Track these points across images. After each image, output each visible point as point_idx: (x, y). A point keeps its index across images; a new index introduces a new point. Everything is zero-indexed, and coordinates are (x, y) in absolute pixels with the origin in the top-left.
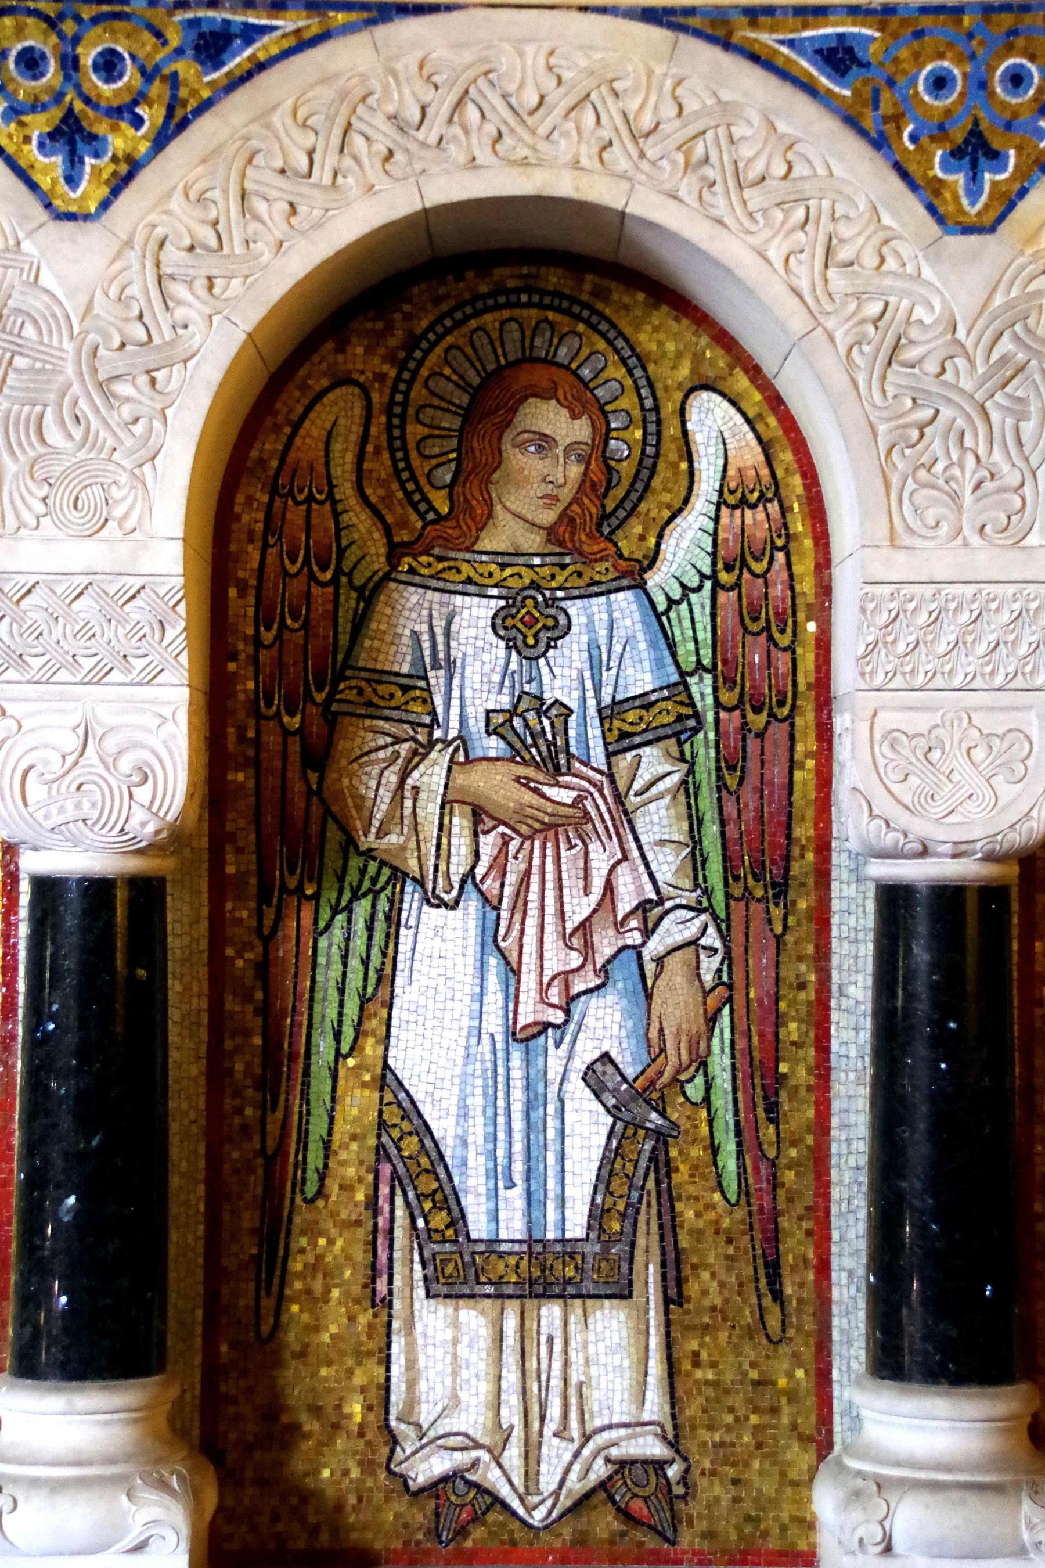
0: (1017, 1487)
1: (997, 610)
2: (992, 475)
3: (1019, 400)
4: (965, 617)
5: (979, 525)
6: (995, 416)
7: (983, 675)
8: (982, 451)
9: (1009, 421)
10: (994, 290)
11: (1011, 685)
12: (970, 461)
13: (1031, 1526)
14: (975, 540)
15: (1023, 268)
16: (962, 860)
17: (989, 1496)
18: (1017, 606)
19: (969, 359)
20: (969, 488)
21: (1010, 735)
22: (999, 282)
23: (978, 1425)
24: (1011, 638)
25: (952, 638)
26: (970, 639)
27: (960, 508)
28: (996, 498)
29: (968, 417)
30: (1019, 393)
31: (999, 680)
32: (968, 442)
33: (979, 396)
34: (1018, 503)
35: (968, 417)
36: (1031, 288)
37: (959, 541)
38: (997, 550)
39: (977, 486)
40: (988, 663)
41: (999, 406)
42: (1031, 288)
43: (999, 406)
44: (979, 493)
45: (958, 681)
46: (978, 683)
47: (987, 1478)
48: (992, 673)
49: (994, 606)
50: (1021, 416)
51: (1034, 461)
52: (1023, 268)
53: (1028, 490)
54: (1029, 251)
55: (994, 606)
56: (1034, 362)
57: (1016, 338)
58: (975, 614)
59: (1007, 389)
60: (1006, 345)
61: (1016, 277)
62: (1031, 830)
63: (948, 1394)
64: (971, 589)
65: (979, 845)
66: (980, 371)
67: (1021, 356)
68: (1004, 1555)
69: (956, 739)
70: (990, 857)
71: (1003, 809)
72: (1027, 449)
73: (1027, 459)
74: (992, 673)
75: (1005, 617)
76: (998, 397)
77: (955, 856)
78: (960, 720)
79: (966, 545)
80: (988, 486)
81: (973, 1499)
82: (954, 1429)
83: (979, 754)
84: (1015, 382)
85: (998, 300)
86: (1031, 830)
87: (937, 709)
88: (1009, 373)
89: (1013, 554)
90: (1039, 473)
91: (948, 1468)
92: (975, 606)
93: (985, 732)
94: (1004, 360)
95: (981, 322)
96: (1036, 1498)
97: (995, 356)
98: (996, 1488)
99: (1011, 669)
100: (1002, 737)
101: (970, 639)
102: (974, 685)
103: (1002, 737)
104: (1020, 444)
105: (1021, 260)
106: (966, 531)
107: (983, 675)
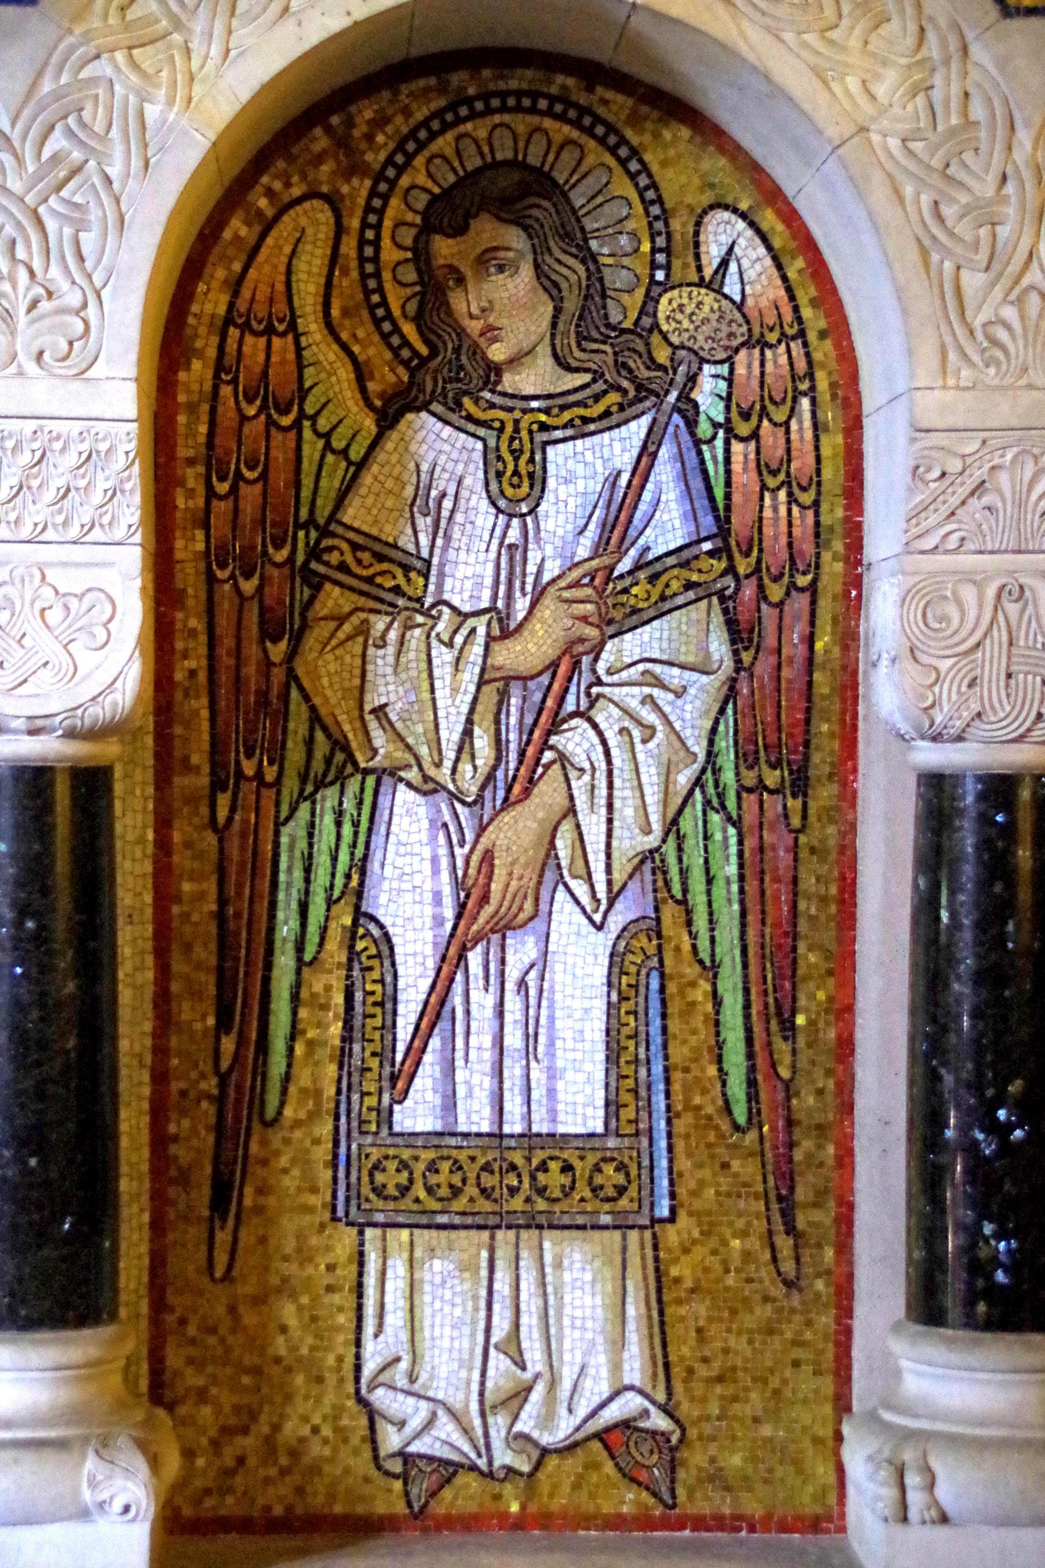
0: (85, 1440)
1: (63, 450)
2: (50, 294)
3: (76, 206)
4: (25, 458)
5: (35, 350)
6: (51, 225)
7: (55, 525)
8: (37, 265)
9: (67, 231)
10: (40, 74)
11: (87, 539)
12: (23, 275)
13: (93, 1484)
14: (31, 367)
15: (72, 49)
16: (42, 737)
17: (48, 1454)
18: (85, 447)
19: (15, 155)
20: (23, 308)
21: (89, 595)
22: (46, 64)
23: (49, 1374)
24: (82, 483)
25: (14, 481)
26: (35, 483)
27: (13, 333)
28: (57, 319)
29: (19, 224)
30: (78, 199)
31: (74, 532)
32: (21, 253)
33: (30, 199)
34: (80, 327)
35: (19, 224)
36: (83, 75)
37: (13, 369)
38: (57, 382)
39: (34, 304)
40: (60, 511)
41: (53, 212)
42: (83, 75)
43: (53, 212)
44: (35, 313)
45: (25, 532)
46: (50, 535)
47: (52, 1434)
48: (65, 523)
49: (58, 445)
50: (81, 227)
51: (98, 279)
52: (72, 49)
53: (92, 311)
54: (78, 30)
55: (58, 445)
56: (92, 163)
57: (70, 133)
58: (38, 454)
59: (64, 193)
60: (57, 142)
61: (65, 61)
62: (115, 704)
63: (13, 1342)
64: (31, 425)
65: (58, 719)
66: (31, 169)
67: (77, 155)
68: (62, 1519)
69: (28, 597)
70: (71, 734)
71: (84, 679)
72: (89, 264)
73: (89, 277)
74: (65, 523)
75: (72, 459)
76: (53, 201)
77: (32, 732)
78: (31, 576)
79: (21, 373)
80: (45, 306)
81: (28, 1457)
82: (22, 1380)
83: (54, 616)
84: (72, 185)
85: (47, 86)
86: (115, 704)
87: (7, 563)
88: (62, 174)
89: (77, 385)
90: (105, 294)
91: (23, 1424)
92: (36, 445)
93: (62, 591)
94: (56, 159)
95: (26, 113)
96: (104, 1452)
97: (46, 153)
98: (60, 1445)
99: (86, 519)
100: (80, 597)
101: (35, 483)
102: (44, 537)
103: (80, 597)
104: (81, 259)
105: (71, 40)
106: (21, 357)
107: (55, 525)
